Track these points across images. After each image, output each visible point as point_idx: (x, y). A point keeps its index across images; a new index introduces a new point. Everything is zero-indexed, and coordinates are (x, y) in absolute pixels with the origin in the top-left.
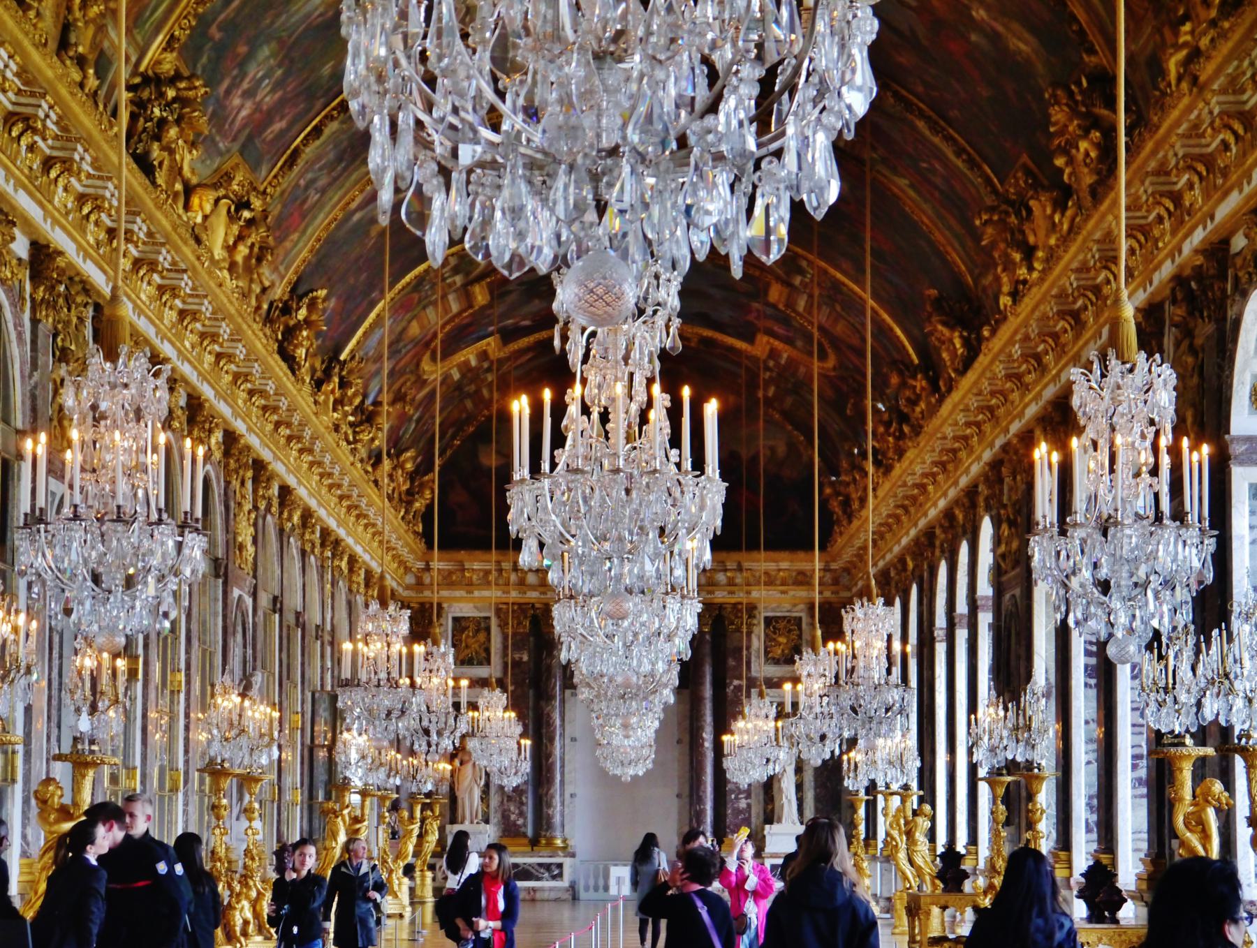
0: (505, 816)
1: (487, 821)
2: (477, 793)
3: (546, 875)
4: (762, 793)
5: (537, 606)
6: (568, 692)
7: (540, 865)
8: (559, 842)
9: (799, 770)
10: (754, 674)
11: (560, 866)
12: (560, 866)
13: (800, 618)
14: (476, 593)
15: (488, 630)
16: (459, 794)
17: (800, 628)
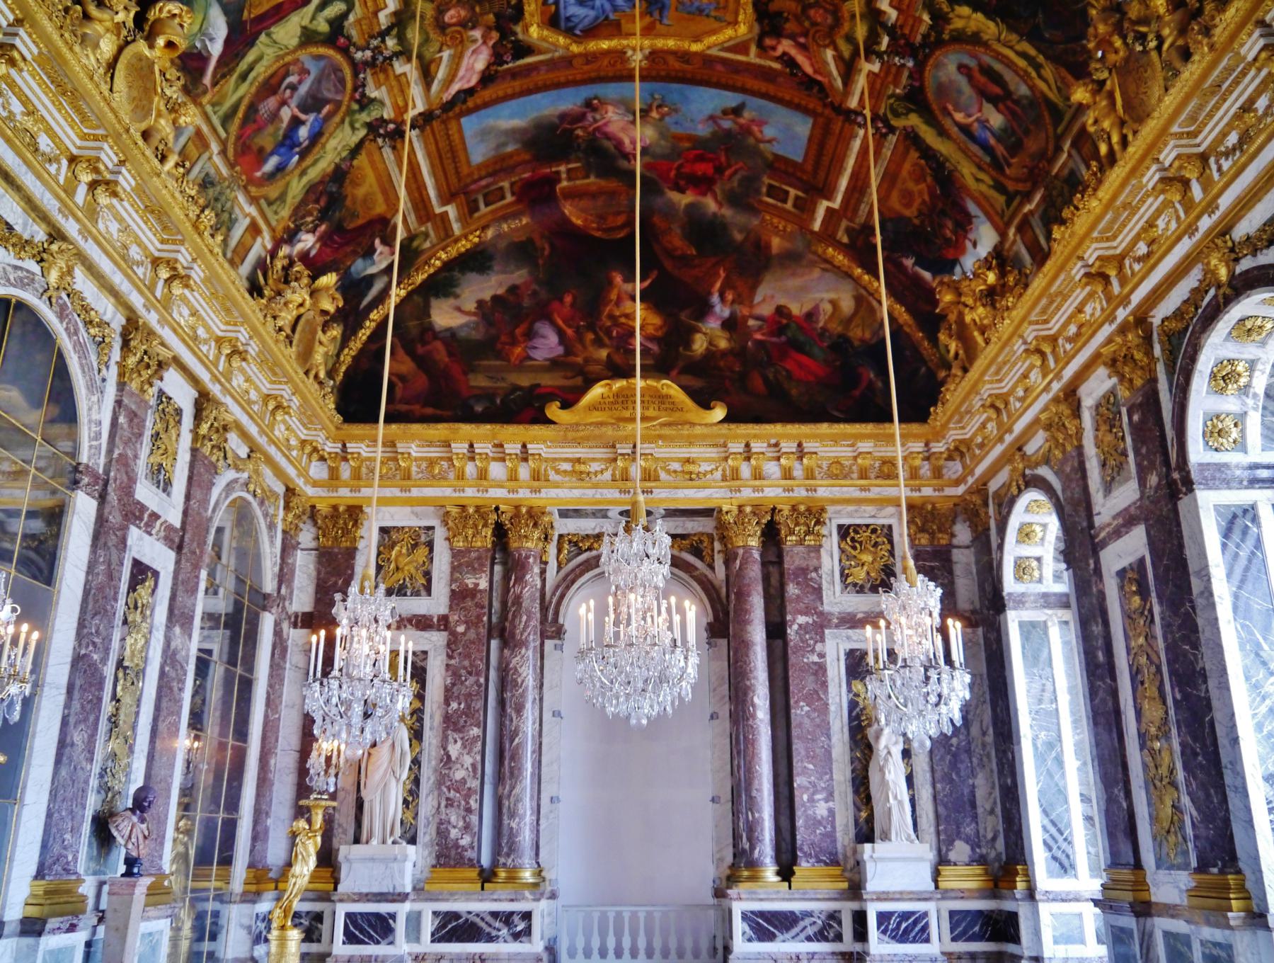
0: (442, 833)
1: (413, 841)
2: (396, 794)
3: (504, 931)
4: (850, 790)
5: (503, 508)
6: (549, 644)
7: (495, 915)
8: (527, 875)
9: (906, 754)
10: (827, 608)
11: (527, 916)
12: (527, 916)
13: (890, 527)
14: (415, 492)
15: (430, 545)
16: (363, 793)
17: (891, 542)
